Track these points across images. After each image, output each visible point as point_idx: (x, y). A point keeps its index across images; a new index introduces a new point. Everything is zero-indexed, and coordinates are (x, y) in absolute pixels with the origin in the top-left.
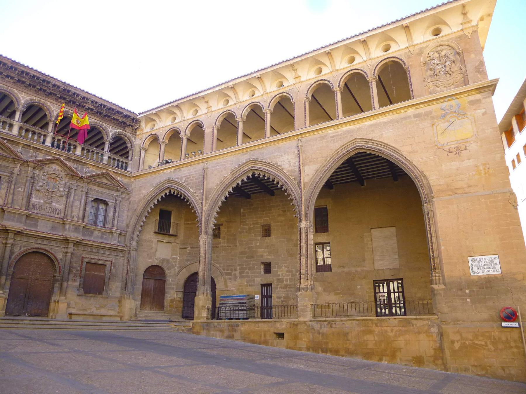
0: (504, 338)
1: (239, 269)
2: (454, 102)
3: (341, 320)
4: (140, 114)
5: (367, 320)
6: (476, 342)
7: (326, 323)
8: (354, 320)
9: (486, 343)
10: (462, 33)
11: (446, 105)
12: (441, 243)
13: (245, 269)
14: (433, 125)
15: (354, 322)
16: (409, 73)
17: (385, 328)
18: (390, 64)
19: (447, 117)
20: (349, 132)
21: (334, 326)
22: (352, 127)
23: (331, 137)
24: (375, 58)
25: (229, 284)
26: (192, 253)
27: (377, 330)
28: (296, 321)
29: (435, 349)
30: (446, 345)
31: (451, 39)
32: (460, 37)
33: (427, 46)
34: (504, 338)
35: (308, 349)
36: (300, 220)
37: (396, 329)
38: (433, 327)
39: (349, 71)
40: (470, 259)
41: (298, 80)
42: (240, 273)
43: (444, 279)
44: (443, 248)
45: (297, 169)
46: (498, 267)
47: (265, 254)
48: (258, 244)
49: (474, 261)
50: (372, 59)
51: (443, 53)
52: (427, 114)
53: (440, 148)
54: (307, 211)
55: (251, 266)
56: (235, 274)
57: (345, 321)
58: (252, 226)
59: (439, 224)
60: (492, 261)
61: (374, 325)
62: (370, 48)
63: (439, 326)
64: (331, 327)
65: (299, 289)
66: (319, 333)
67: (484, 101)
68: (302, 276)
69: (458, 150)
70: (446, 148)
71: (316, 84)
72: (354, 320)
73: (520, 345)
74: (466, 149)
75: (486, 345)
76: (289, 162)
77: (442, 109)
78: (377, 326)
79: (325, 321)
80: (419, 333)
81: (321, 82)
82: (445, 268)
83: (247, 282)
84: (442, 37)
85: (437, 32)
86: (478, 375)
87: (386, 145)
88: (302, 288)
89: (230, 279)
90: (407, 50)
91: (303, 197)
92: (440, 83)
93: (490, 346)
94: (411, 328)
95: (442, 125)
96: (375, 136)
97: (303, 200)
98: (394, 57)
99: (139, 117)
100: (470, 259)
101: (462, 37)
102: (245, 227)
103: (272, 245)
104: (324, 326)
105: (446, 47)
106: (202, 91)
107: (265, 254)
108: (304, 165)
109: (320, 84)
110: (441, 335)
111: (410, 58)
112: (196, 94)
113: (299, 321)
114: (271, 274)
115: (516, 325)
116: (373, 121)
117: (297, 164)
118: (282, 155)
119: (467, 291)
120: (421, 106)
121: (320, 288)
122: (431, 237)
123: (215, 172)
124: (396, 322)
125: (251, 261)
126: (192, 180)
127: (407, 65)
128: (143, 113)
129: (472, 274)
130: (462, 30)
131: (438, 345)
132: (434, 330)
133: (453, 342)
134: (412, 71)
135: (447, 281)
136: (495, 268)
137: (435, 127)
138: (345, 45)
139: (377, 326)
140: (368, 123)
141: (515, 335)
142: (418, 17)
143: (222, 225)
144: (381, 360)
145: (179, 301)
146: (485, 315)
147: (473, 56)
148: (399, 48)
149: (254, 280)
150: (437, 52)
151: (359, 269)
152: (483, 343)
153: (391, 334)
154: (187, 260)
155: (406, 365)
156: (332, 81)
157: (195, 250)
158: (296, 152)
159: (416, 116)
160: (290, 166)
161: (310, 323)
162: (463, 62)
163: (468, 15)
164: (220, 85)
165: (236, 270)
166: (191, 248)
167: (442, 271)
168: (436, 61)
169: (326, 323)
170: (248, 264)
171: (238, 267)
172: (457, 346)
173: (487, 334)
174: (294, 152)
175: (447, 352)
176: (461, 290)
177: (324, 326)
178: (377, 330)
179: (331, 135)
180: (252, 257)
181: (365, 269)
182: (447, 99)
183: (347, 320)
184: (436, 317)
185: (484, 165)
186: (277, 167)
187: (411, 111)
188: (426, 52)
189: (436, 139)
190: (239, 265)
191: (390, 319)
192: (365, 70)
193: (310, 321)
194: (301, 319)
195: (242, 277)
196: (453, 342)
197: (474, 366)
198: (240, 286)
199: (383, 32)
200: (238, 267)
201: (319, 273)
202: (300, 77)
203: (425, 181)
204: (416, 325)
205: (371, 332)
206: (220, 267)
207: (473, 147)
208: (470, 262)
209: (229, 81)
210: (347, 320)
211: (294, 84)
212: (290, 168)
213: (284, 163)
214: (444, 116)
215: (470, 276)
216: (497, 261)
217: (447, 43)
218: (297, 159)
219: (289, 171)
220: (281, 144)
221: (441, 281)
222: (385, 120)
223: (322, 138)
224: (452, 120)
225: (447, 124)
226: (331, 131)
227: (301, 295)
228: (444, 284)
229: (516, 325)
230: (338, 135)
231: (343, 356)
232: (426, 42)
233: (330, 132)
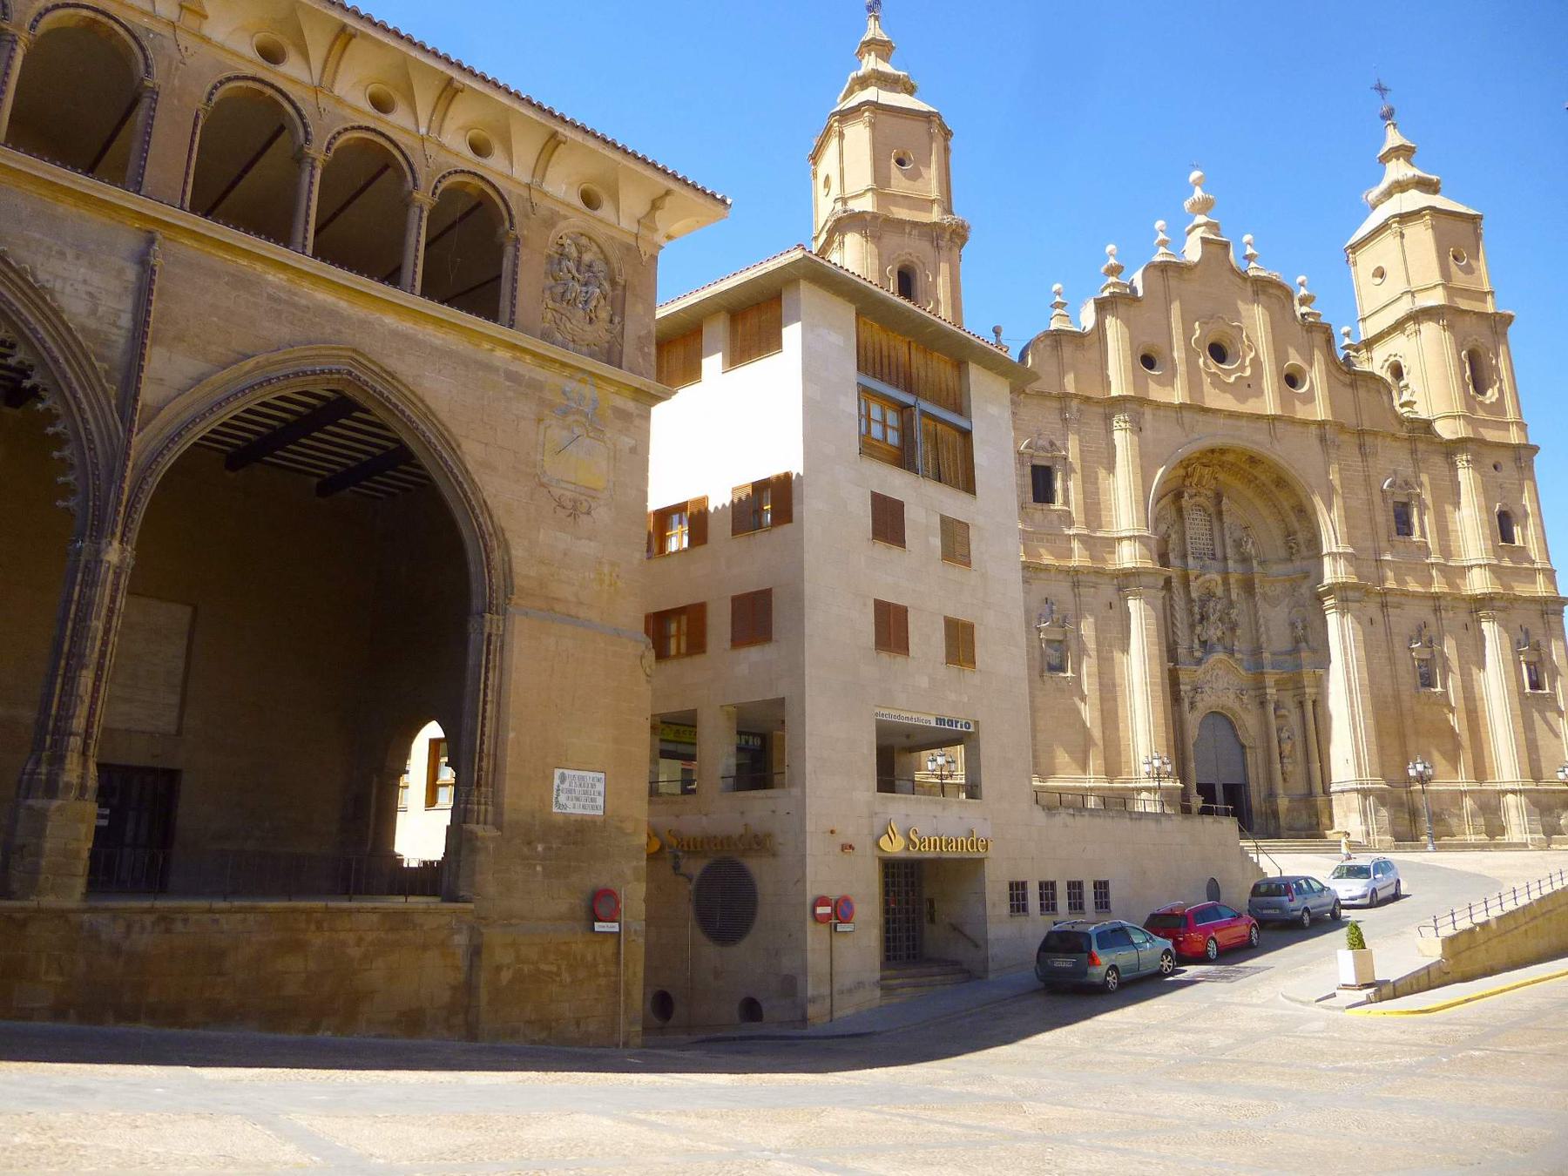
0: (589, 958)
2: (588, 391)
3: (210, 911)
5: (294, 910)
6: (544, 967)
7: (148, 919)
8: (253, 910)
9: (559, 967)
10: (632, 241)
11: (571, 386)
12: (512, 722)
14: (540, 421)
15: (251, 917)
16: (516, 257)
17: (342, 935)
18: (468, 190)
19: (571, 418)
20: (332, 314)
21: (179, 926)
22: (343, 304)
23: (270, 297)
24: (449, 151)
27: (317, 940)
28: (23, 909)
29: (454, 988)
30: (484, 977)
31: (612, 238)
32: (628, 248)
33: (566, 218)
34: (589, 958)
35: (59, 1013)
36: (99, 530)
37: (370, 937)
38: (459, 931)
39: (367, 129)
40: (558, 772)
41: (190, 21)
43: (499, 812)
44: (512, 735)
45: (120, 338)
46: (600, 801)
49: (563, 778)
50: (441, 146)
51: (587, 257)
52: (536, 386)
53: (542, 485)
54: (131, 506)
57: (222, 911)
59: (514, 676)
60: (593, 786)
61: (313, 927)
62: (450, 114)
63: (472, 929)
64: (168, 931)
65: (51, 789)
66: (116, 951)
67: (637, 422)
68: (75, 742)
69: (575, 508)
70: (557, 492)
71: (251, 84)
72: (253, 910)
73: (613, 969)
74: (589, 513)
75: (559, 975)
76: (90, 294)
77: (564, 393)
78: (319, 928)
79: (150, 911)
80: (425, 947)
81: (269, 91)
82: (509, 787)
84: (600, 221)
85: (590, 200)
86: (533, 1042)
87: (429, 414)
88: (68, 786)
90: (525, 194)
91: (132, 453)
92: (568, 325)
93: (566, 977)
94: (410, 934)
95: (556, 433)
96: (405, 367)
97: (130, 464)
98: (493, 186)
100: (558, 772)
101: (631, 251)
104: (143, 928)
105: (595, 248)
108: (155, 341)
109: (261, 93)
110: (476, 951)
111: (527, 216)
113: (39, 910)
115: (614, 927)
116: (406, 326)
117: (126, 320)
118: (62, 254)
119: (540, 848)
120: (528, 358)
122: (485, 703)
124: (375, 918)
129: (555, 810)
131: (462, 977)
132: (461, 939)
133: (499, 969)
134: (524, 254)
135: (506, 817)
136: (593, 800)
137: (542, 427)
138: (406, 57)
139: (319, 928)
140: (390, 320)
141: (609, 948)
142: (591, 143)
144: (314, 1028)
146: (562, 907)
147: (640, 308)
148: (509, 170)
150: (577, 245)
152: (554, 969)
153: (355, 952)
155: (380, 1036)
156: (308, 120)
158: (131, 273)
159: (512, 377)
160: (93, 312)
161: (86, 916)
162: (619, 308)
163: (658, 213)
167: (497, 793)
168: (571, 265)
169: (148, 919)
172: (506, 976)
173: (563, 948)
174: (121, 271)
175: (484, 995)
176: (529, 843)
177: (143, 928)
178: (317, 940)
179: (270, 290)
182: (580, 375)
183: (229, 911)
184: (471, 906)
185: (612, 564)
187: (502, 354)
188: (562, 227)
189: (539, 457)
191: (359, 911)
192: (416, 166)
193: (85, 911)
194: (49, 901)
196: (499, 969)
197: (530, 1022)
199: (508, 109)
202: (206, 17)
203: (497, 556)
204: (421, 926)
205: (298, 946)
207: (602, 514)
208: (557, 781)
210: (229, 911)
211: (172, 24)
212: (92, 324)
213: (68, 289)
214: (565, 412)
215: (550, 813)
216: (600, 787)
217: (601, 241)
218: (127, 304)
219: (83, 329)
220: (65, 208)
221: (490, 817)
222: (438, 342)
223: (240, 282)
224: (578, 431)
225: (565, 433)
226: (274, 277)
227: (59, 809)
228: (499, 826)
229: (614, 927)
230: (295, 305)
231: (195, 1026)
232: (568, 205)
233: (270, 277)
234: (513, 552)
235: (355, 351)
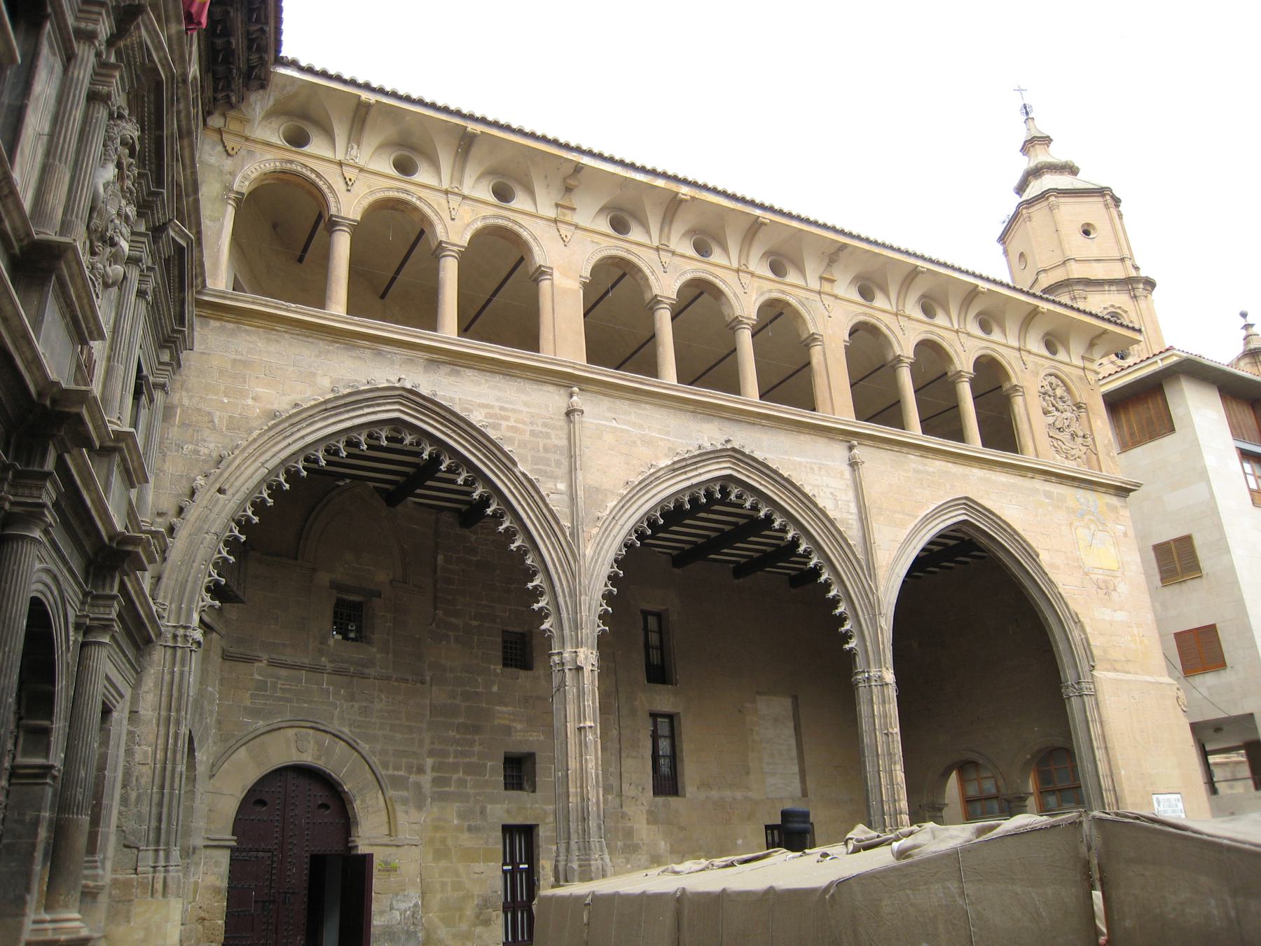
1: (433, 769)
4: (294, 64)
13: (454, 768)
25: (402, 818)
26: (274, 685)
42: (435, 781)
47: (519, 726)
48: (495, 689)
55: (474, 760)
56: (418, 786)
58: (475, 623)
70: (1095, 577)
83: (462, 816)
87: (1013, 534)
89: (405, 801)
99: (282, 71)
102: (453, 620)
103: (538, 698)
106: (590, 153)
107: (519, 726)
112: (567, 147)
114: (538, 794)
121: (662, 843)
123: (609, 438)
125: (472, 743)
126: (513, 429)
127: (1014, 381)
128: (310, 70)
130: (1084, 369)
143: (379, 596)
145: (217, 890)
149: (483, 812)
151: (739, 795)
154: (255, 713)
157: (283, 672)
164: (653, 172)
165: (421, 770)
166: (272, 663)
170: (464, 754)
171: (429, 762)
180: (476, 729)
181: (750, 794)
186: (808, 502)
190: (431, 753)
195: (442, 797)
198: (437, 829)
200: (429, 762)
201: (660, 800)
206: (374, 753)
209: (685, 182)
234: (1088, 630)
235: (966, 498)
